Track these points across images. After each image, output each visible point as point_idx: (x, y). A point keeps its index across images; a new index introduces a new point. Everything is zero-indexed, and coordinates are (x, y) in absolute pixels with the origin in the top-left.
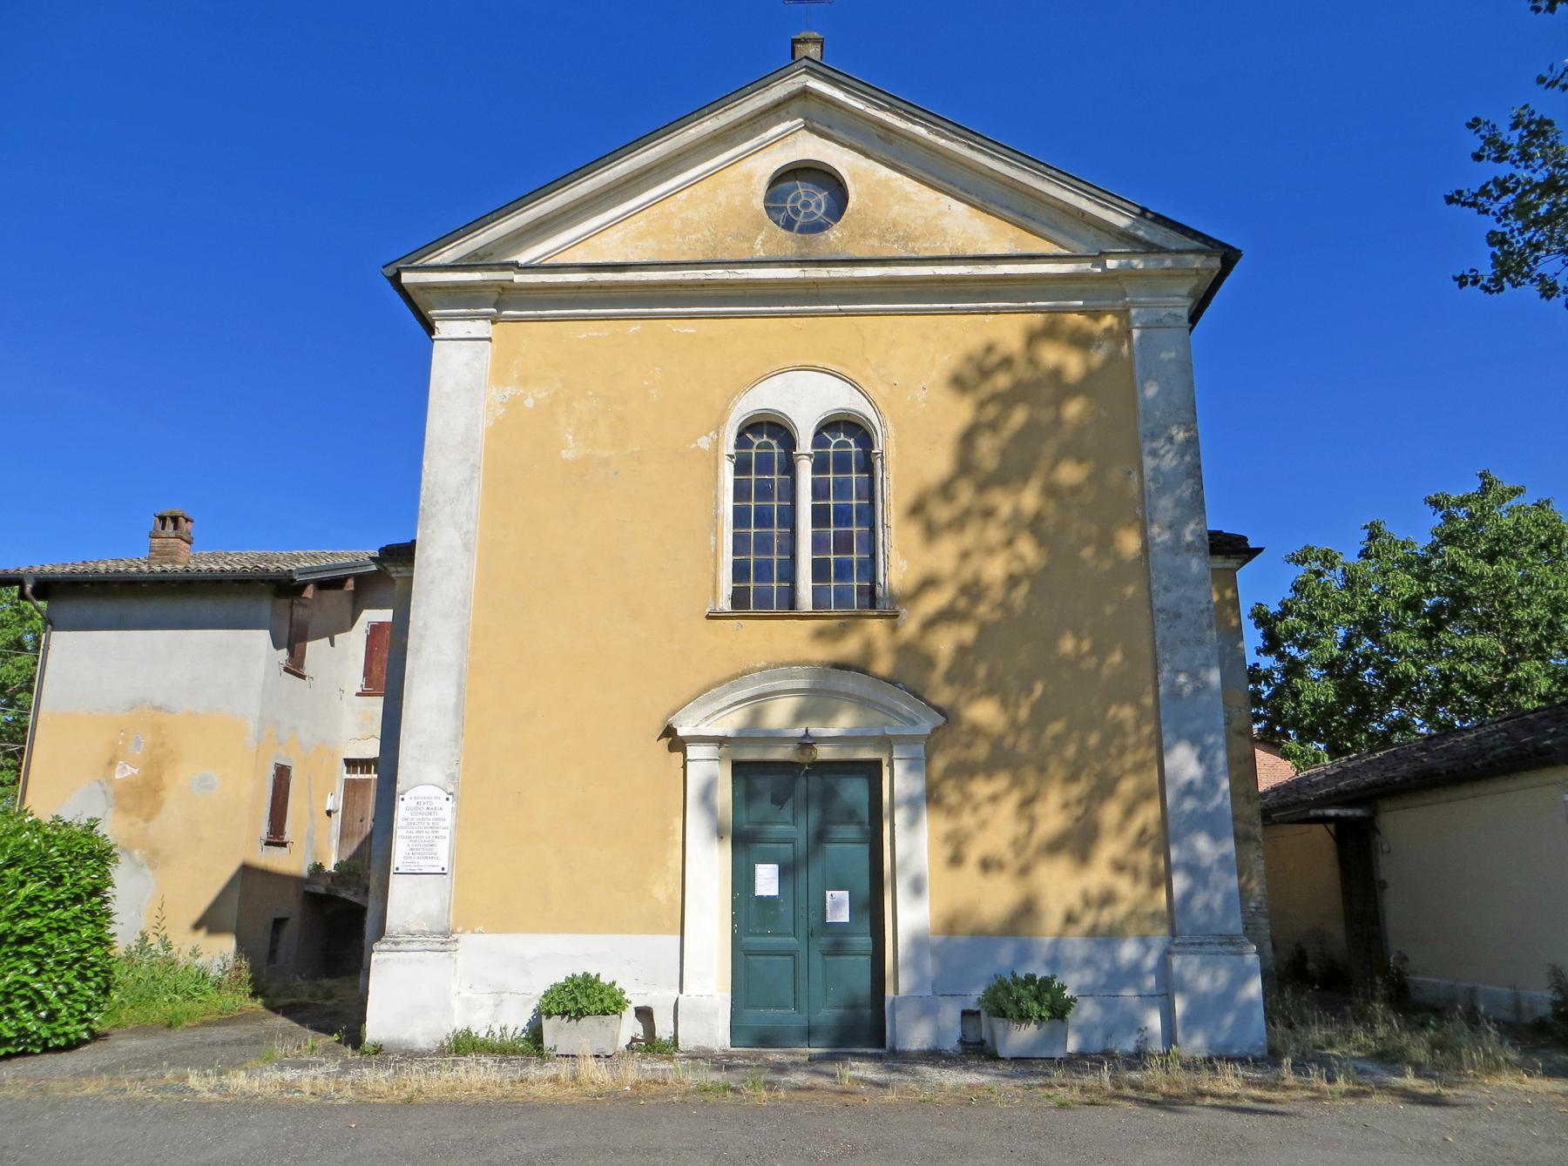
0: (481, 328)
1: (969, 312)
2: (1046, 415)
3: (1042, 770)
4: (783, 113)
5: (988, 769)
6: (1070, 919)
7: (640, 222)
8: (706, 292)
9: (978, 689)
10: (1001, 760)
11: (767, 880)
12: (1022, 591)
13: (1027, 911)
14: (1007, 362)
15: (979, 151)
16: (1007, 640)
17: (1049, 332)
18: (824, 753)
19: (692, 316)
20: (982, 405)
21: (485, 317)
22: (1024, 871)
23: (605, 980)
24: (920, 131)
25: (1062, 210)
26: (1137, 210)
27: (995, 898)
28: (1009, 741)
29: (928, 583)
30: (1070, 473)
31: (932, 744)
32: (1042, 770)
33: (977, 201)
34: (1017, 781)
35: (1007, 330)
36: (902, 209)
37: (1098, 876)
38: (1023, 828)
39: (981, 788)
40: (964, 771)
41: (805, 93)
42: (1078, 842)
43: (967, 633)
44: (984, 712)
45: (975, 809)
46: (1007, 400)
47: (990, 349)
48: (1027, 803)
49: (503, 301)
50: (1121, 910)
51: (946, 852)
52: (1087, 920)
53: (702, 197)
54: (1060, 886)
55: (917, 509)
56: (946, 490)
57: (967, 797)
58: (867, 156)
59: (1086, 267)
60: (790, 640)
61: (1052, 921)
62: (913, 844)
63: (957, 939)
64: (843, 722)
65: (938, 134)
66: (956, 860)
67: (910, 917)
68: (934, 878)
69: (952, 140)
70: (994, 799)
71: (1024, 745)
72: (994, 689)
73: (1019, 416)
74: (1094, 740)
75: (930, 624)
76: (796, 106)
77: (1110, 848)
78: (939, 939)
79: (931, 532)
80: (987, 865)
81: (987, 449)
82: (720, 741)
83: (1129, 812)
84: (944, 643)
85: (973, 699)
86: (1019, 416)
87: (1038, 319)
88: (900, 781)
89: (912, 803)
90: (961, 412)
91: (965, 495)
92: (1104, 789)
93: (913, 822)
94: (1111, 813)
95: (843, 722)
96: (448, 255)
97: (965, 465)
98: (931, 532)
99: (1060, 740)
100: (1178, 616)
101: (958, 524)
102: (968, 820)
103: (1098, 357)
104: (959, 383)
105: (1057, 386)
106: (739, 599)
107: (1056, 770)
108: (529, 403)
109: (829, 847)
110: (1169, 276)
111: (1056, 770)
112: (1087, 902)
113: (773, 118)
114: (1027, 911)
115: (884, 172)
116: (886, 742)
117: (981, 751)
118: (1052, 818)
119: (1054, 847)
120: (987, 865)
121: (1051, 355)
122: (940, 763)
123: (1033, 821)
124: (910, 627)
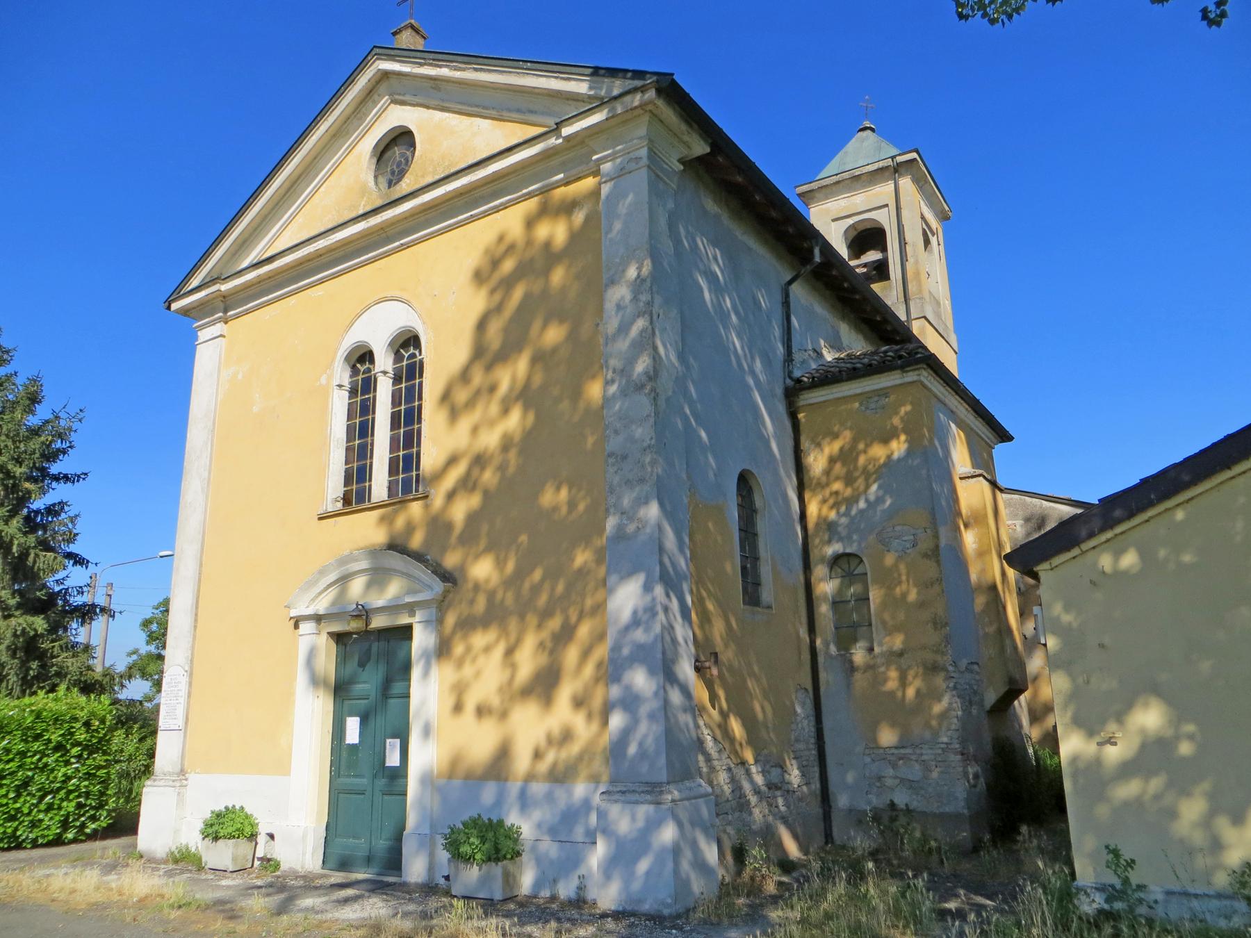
0: (218, 328)
1: (485, 214)
2: (537, 287)
3: (522, 617)
4: (376, 97)
5: (484, 622)
6: (537, 755)
7: (299, 219)
8: (325, 259)
9: (482, 547)
10: (493, 616)
11: (353, 727)
12: (512, 455)
13: (503, 754)
14: (511, 248)
15: (481, 70)
16: (506, 502)
17: (545, 211)
18: (378, 622)
19: (321, 281)
20: (492, 292)
21: (219, 320)
22: (504, 715)
23: (248, 810)
24: (445, 72)
25: (550, 95)
26: (589, 71)
27: (479, 741)
28: (499, 596)
29: (452, 461)
30: (554, 335)
31: (442, 605)
32: (522, 617)
33: (494, 113)
34: (504, 631)
35: (510, 220)
36: (454, 140)
37: (563, 712)
38: (507, 673)
39: (479, 639)
40: (468, 625)
41: (386, 75)
42: (544, 685)
43: (475, 501)
44: (483, 569)
45: (474, 660)
46: (508, 284)
47: (501, 238)
48: (510, 652)
49: (226, 306)
50: (575, 748)
51: (450, 702)
52: (550, 757)
53: (337, 187)
54: (530, 727)
55: (446, 397)
56: (464, 376)
57: (468, 649)
58: (428, 107)
59: (553, 141)
60: (366, 529)
61: (522, 762)
62: (427, 691)
63: (461, 778)
64: (394, 589)
65: (456, 69)
66: (458, 708)
67: (424, 757)
68: (449, 720)
69: (464, 70)
70: (487, 649)
71: (510, 599)
72: (495, 547)
73: (518, 293)
74: (560, 588)
75: (451, 496)
76: (383, 88)
77: (565, 693)
78: (443, 781)
79: (454, 415)
80: (482, 711)
81: (495, 329)
82: (318, 618)
83: (585, 654)
84: (459, 512)
85: (477, 557)
86: (518, 293)
87: (532, 204)
88: (421, 639)
89: (426, 656)
90: (478, 302)
91: (478, 378)
92: (565, 635)
93: (426, 673)
94: (571, 655)
95: (394, 589)
96: (195, 282)
97: (479, 351)
98: (454, 415)
99: (536, 590)
100: (624, 457)
101: (470, 404)
102: (468, 670)
103: (579, 217)
104: (479, 277)
105: (550, 256)
106: (347, 500)
107: (532, 620)
108: (240, 377)
109: (392, 701)
110: (625, 122)
111: (532, 620)
112: (550, 741)
113: (370, 104)
114: (503, 754)
115: (438, 115)
116: (411, 608)
117: (481, 604)
118: (528, 662)
119: (526, 692)
120: (482, 711)
121: (543, 231)
122: (450, 620)
123: (513, 667)
124: (438, 501)
